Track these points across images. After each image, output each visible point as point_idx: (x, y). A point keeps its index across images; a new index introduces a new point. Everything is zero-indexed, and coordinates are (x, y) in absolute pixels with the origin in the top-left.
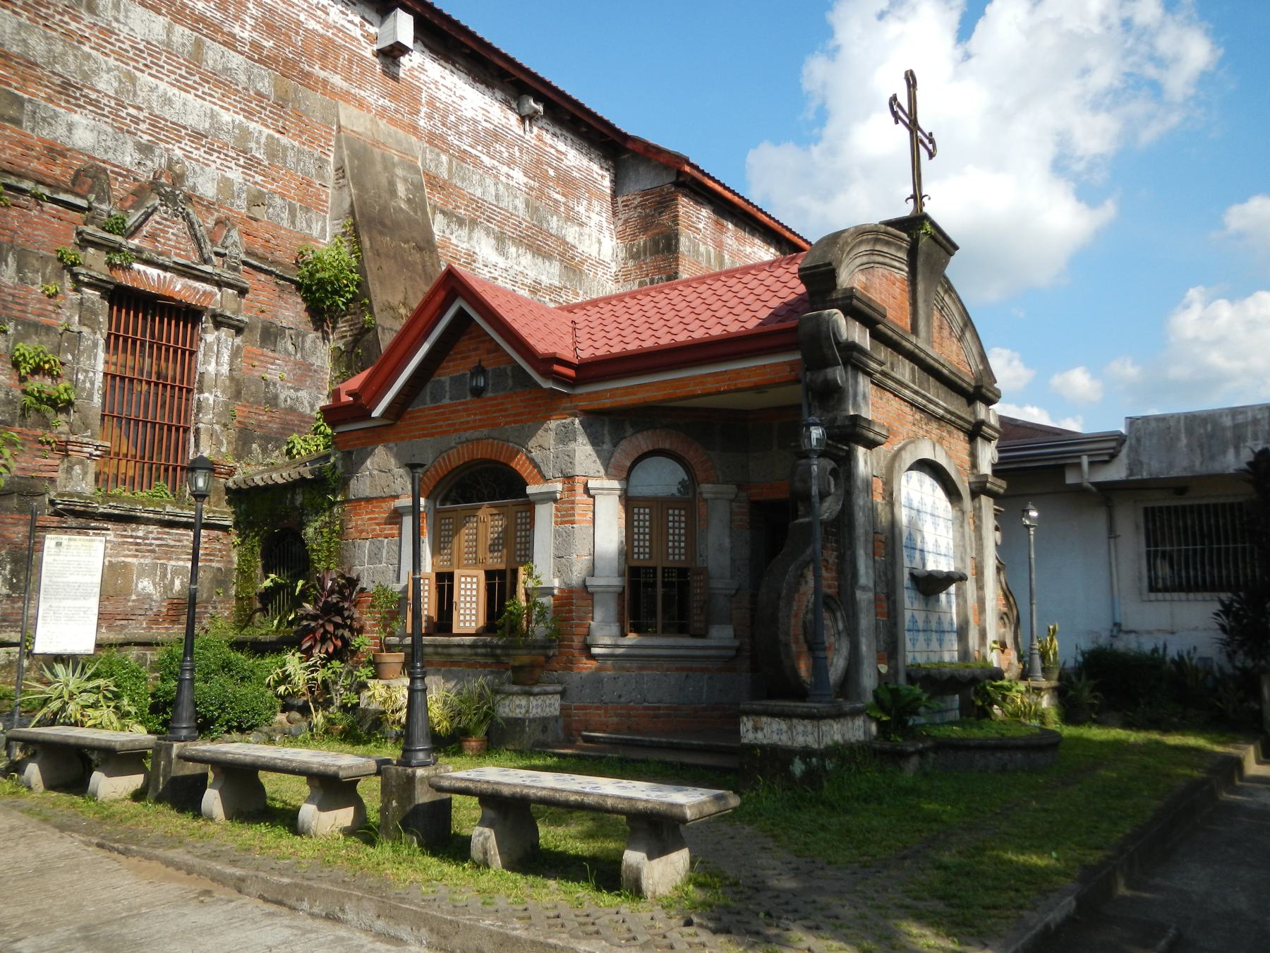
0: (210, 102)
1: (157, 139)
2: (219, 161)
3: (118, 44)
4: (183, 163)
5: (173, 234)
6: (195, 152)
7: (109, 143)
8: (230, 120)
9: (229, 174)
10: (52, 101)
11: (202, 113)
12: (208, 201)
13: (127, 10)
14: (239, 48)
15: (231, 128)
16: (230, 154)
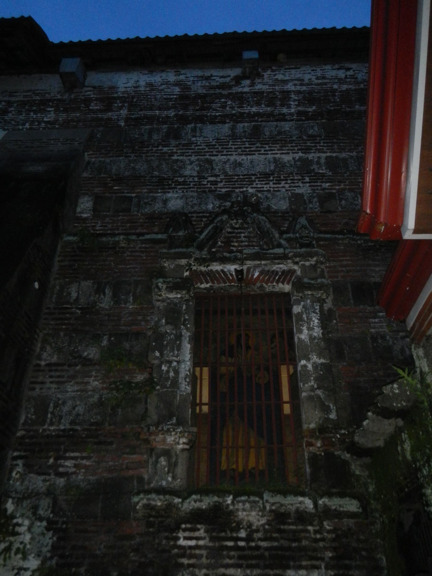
0: (272, 154)
1: (232, 188)
2: (287, 186)
3: (197, 148)
4: (256, 195)
5: (245, 237)
6: (265, 186)
7: (195, 202)
8: (291, 158)
9: (298, 191)
10: (152, 192)
11: (267, 162)
12: (282, 212)
13: (201, 130)
14: (288, 119)
15: (293, 163)
16: (296, 178)
